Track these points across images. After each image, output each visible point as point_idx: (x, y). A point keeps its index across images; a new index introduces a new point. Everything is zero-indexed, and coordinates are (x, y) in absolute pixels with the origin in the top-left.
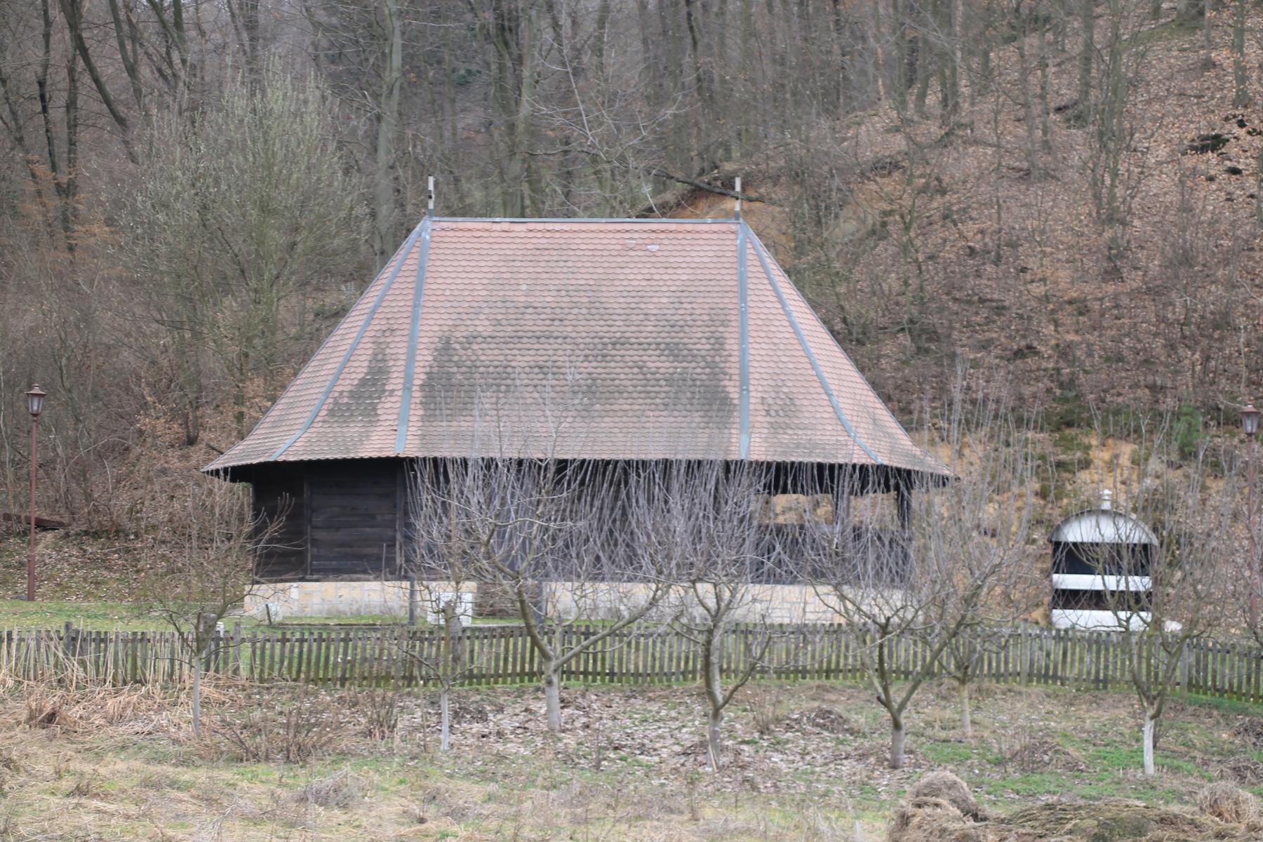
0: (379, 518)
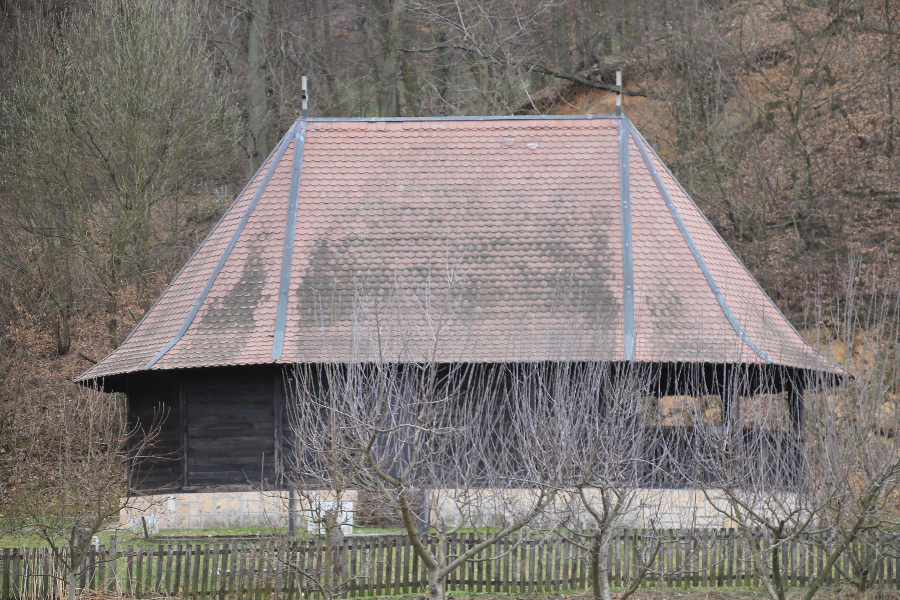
0: (257, 426)
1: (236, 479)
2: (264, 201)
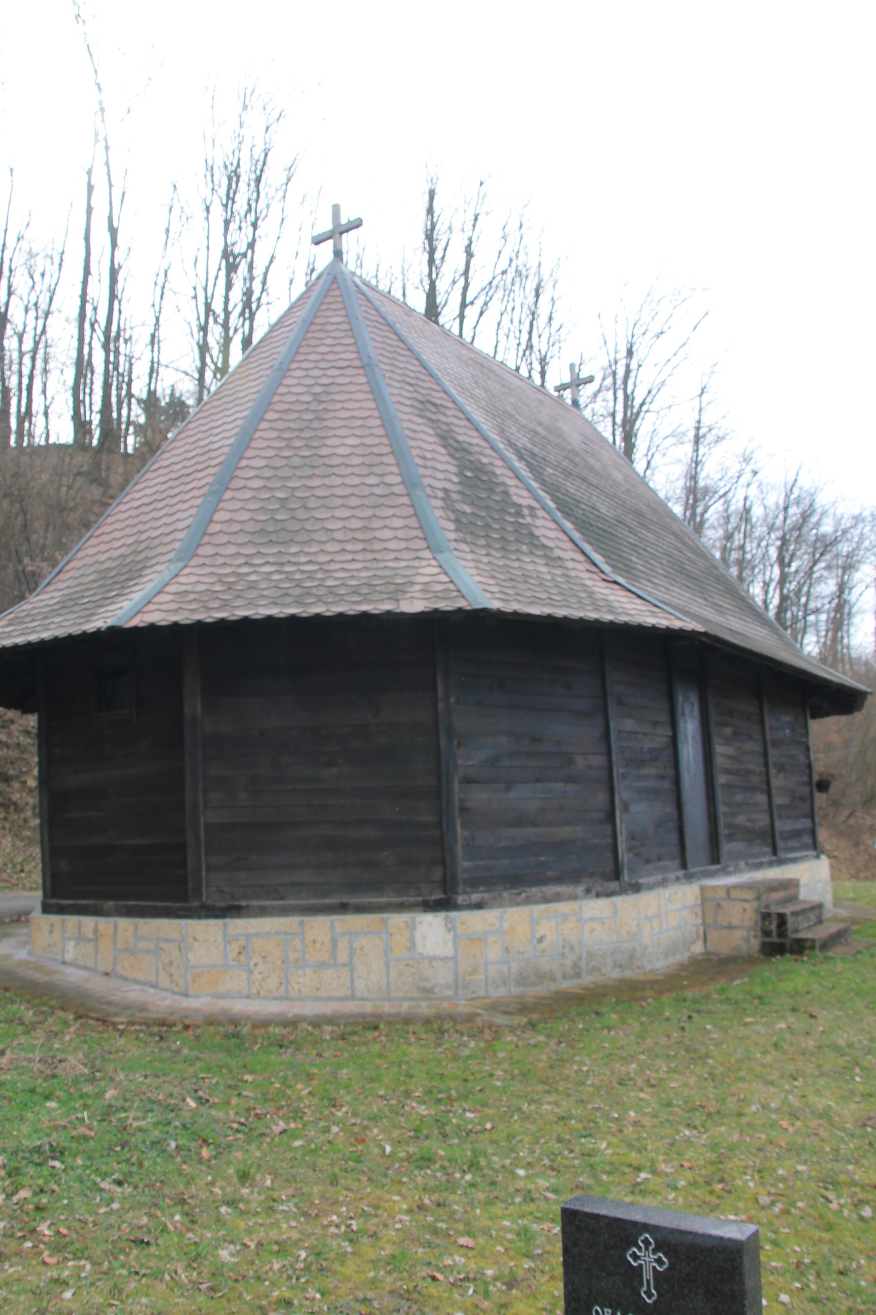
0: (580, 763)
1: (550, 874)
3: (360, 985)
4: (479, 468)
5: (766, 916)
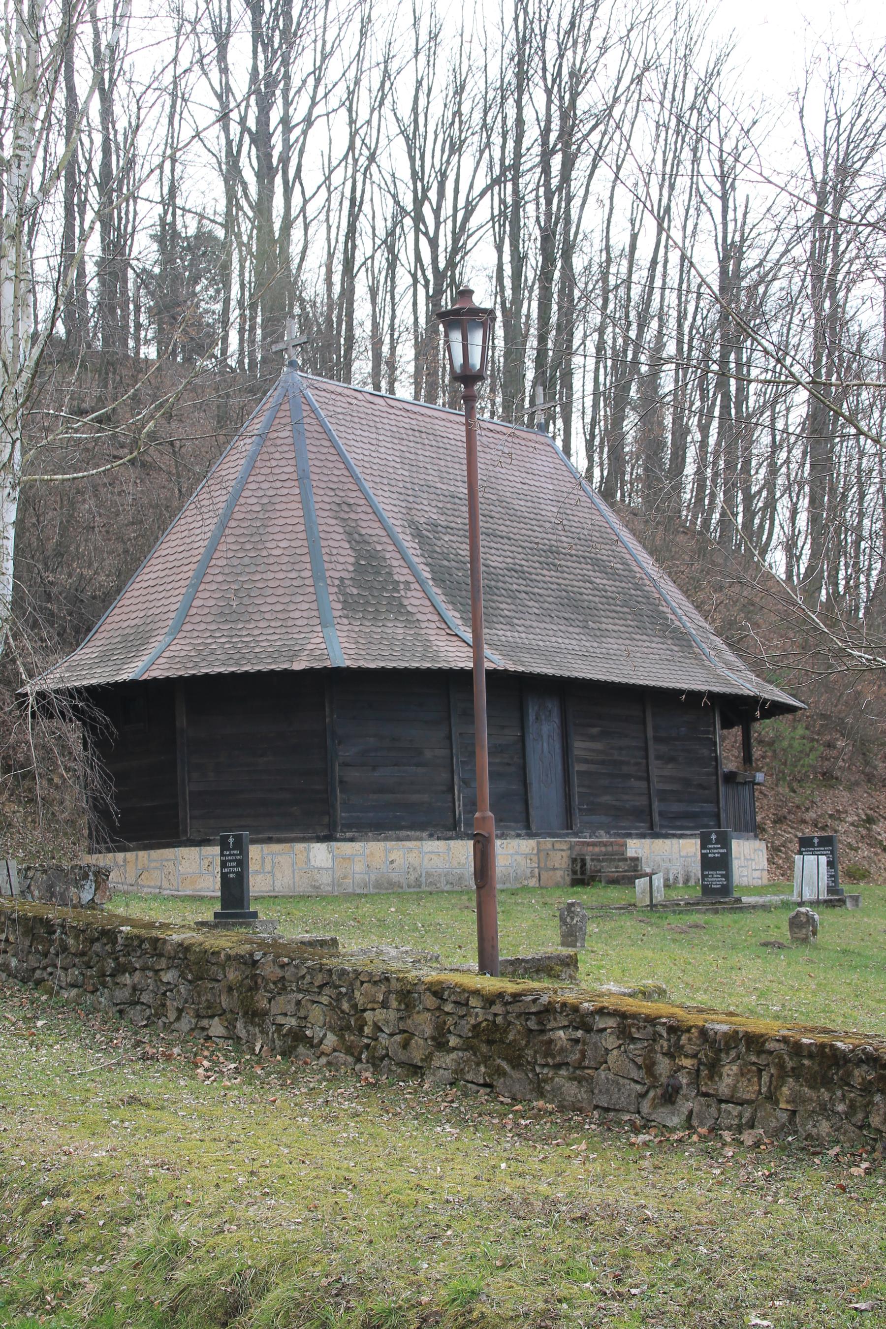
0: (428, 754)
2: (266, 457)
3: (278, 884)
4: (373, 555)
5: (574, 861)
